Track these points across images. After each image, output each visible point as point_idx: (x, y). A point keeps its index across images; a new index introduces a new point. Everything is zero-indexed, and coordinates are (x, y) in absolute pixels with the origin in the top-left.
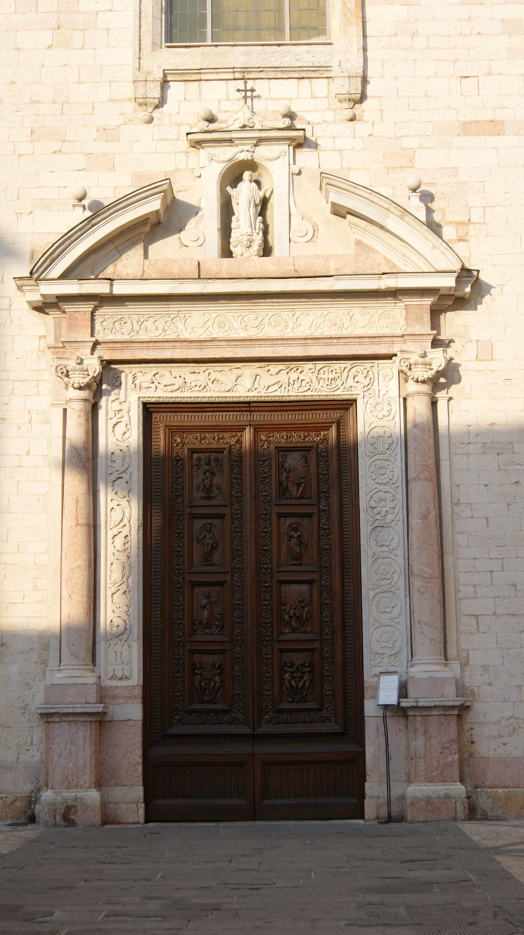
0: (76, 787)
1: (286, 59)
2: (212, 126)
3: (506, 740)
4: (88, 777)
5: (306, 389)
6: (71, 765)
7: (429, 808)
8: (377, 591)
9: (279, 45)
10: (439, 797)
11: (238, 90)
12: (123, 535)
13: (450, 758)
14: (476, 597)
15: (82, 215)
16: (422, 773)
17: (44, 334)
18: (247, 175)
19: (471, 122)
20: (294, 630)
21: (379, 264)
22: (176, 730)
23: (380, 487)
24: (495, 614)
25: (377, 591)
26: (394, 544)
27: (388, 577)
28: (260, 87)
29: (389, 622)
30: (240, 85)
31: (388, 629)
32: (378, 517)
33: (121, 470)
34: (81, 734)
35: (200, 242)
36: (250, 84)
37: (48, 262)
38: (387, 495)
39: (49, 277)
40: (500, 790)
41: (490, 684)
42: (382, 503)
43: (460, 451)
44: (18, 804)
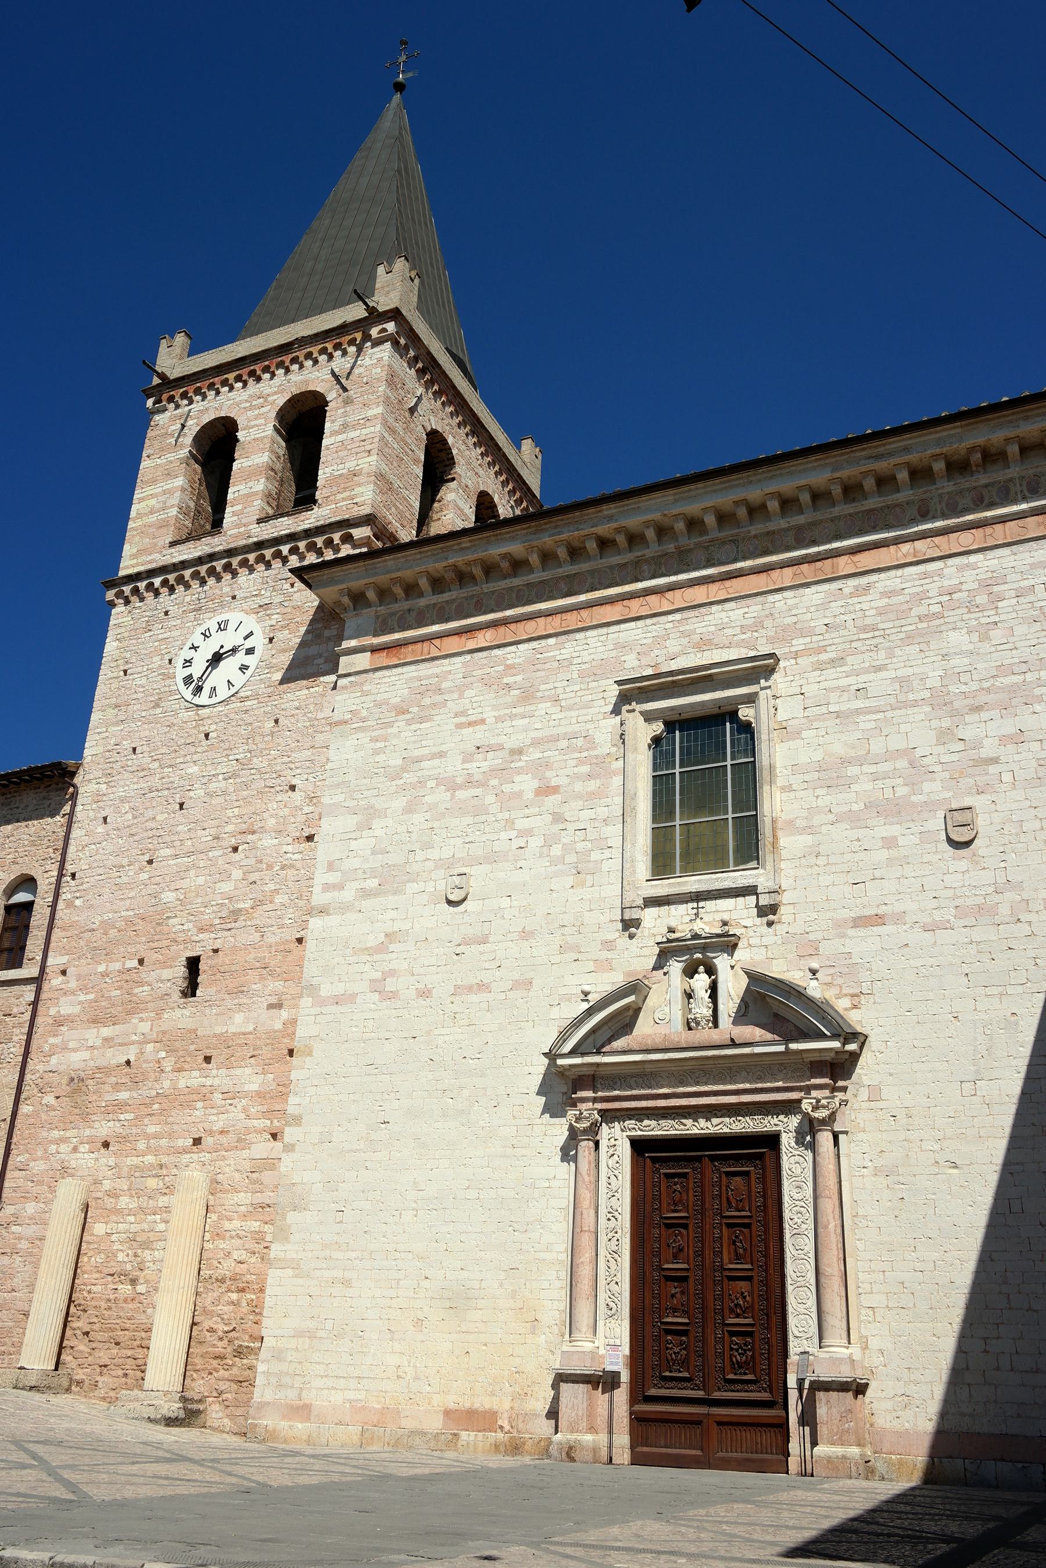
0: (577, 1432)
1: (726, 883)
2: (673, 936)
3: (899, 1413)
4: (584, 1425)
5: (741, 1127)
6: (574, 1414)
7: (830, 1466)
8: (795, 1286)
9: (723, 872)
10: (837, 1457)
11: (693, 908)
12: (615, 1239)
13: (847, 1425)
14: (872, 1293)
15: (585, 1006)
16: (825, 1437)
17: (565, 1090)
18: (701, 969)
19: (859, 918)
20: (738, 1316)
21: (791, 1031)
22: (653, 1392)
23: (797, 1203)
24: (887, 1306)
25: (795, 1286)
26: (806, 1248)
27: (803, 1274)
28: (709, 905)
29: (806, 1312)
30: (695, 905)
31: (803, 1317)
32: (795, 1226)
33: (614, 1190)
34: (580, 1389)
35: (667, 1020)
36: (701, 904)
37: (561, 1042)
38: (802, 1209)
39: (563, 1052)
40: (893, 1457)
41: (885, 1366)
42: (799, 1215)
43: (857, 1174)
44: (542, 1444)
